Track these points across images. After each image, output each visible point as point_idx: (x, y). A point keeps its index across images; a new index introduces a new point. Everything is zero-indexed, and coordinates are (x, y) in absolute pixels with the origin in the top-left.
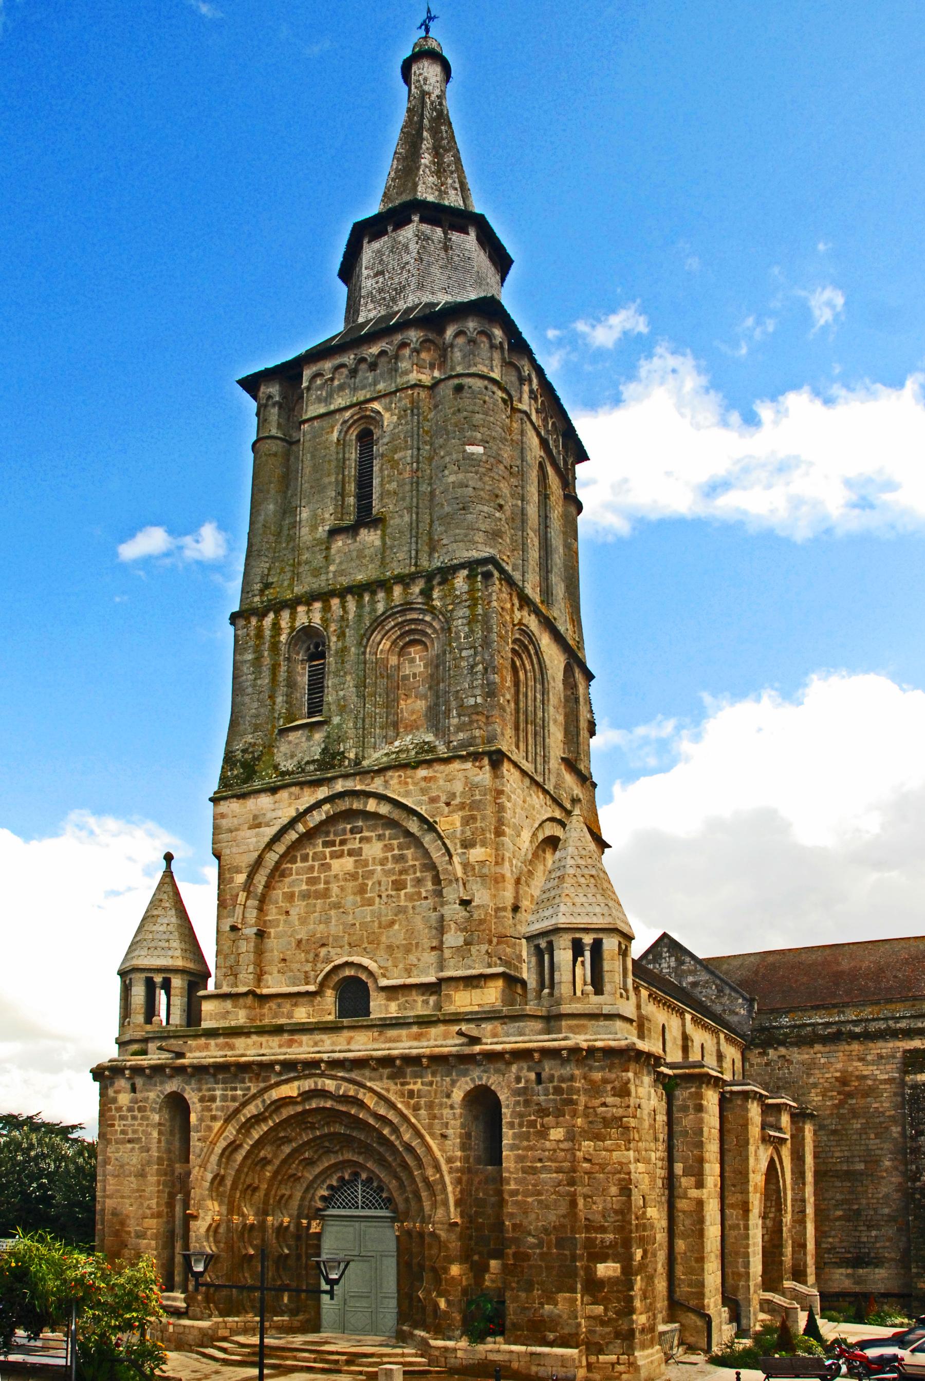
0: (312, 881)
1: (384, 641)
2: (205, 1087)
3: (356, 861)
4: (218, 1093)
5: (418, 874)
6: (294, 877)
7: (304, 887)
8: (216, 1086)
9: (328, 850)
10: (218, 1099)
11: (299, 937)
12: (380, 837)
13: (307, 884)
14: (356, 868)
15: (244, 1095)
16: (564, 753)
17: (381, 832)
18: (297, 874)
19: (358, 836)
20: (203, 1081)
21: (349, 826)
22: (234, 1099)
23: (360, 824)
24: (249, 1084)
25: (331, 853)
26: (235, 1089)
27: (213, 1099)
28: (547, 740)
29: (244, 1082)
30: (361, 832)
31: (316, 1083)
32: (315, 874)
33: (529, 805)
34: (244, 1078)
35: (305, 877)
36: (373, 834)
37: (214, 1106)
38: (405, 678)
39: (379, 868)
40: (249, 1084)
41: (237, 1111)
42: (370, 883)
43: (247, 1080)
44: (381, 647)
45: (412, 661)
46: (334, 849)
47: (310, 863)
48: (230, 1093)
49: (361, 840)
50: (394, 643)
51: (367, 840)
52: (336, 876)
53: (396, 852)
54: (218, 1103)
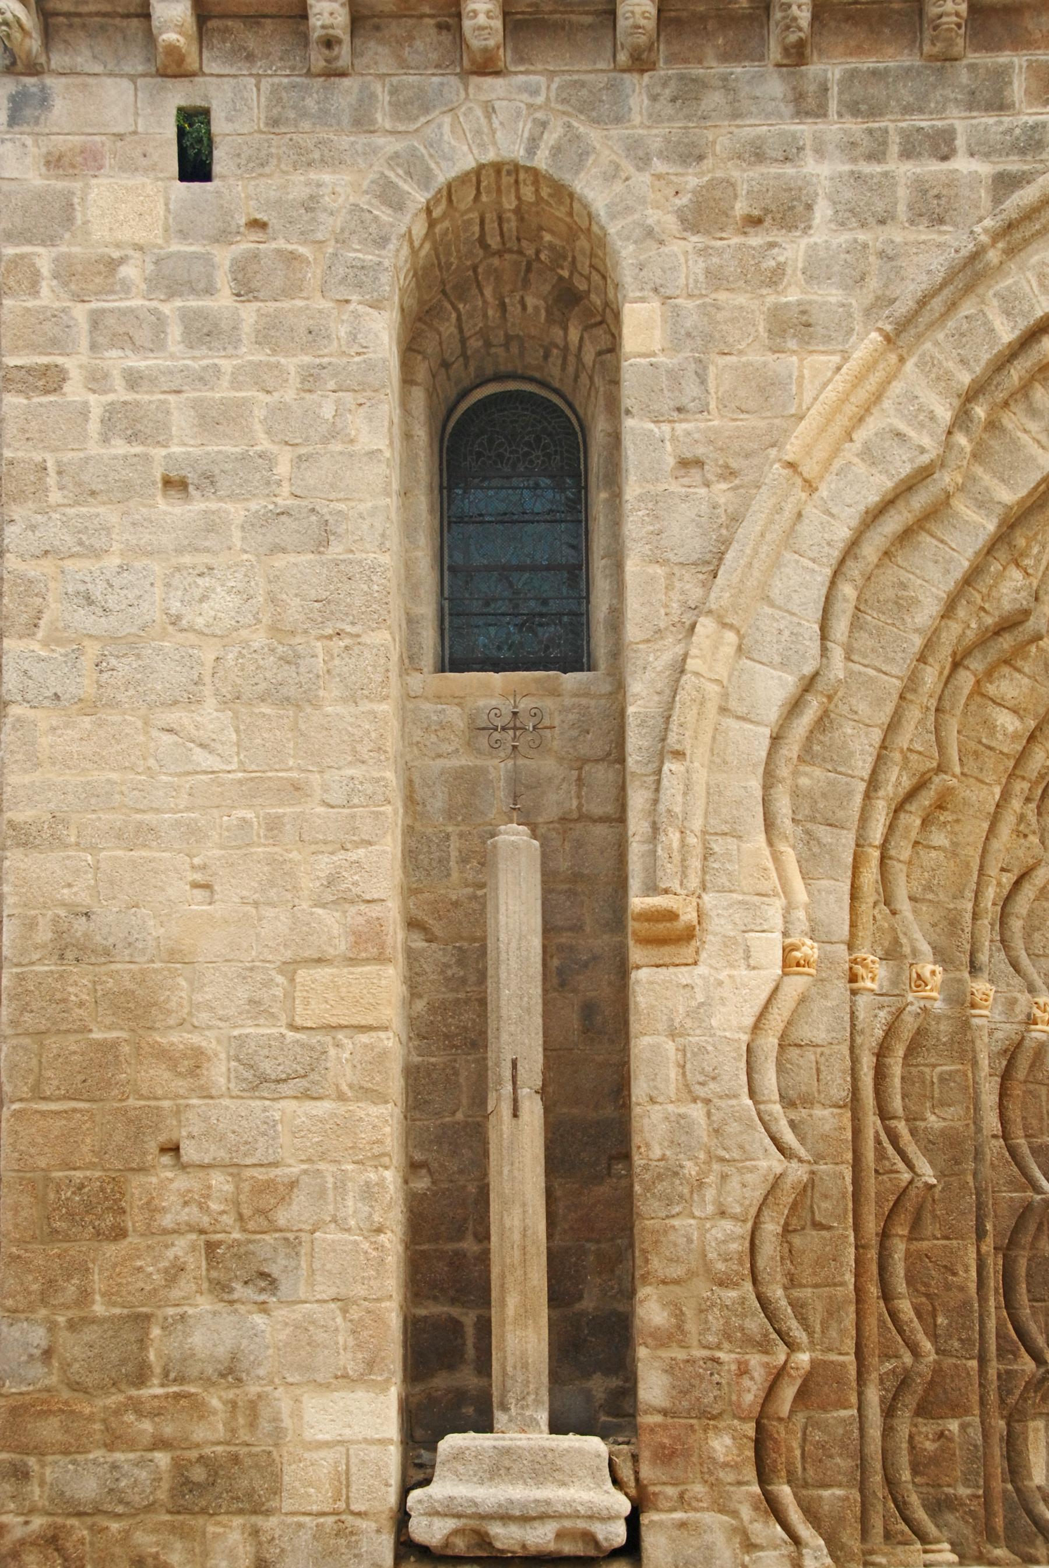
2: (722, 138)
4: (821, 172)
8: (805, 129)
10: (822, 211)
15: (1005, 183)
20: (714, 99)
22: (933, 208)
26: (942, 146)
27: (787, 212)
29: (1000, 105)
34: (1001, 76)
37: (794, 250)
41: (969, 274)
43: (1018, 88)
48: (905, 170)
54: (823, 232)
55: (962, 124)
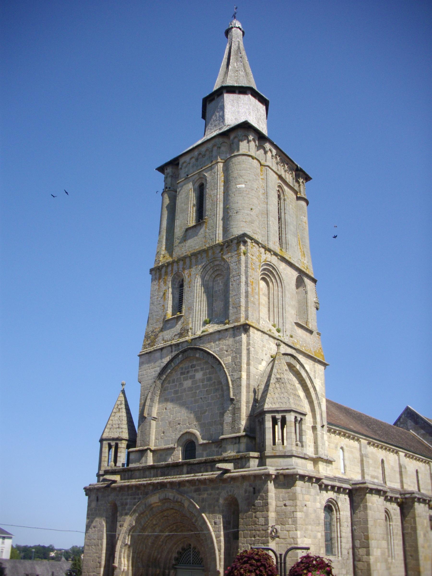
0: (176, 392)
1: (206, 276)
3: (193, 381)
5: (216, 387)
6: (169, 390)
7: (173, 395)
9: (182, 377)
11: (170, 420)
12: (202, 369)
13: (174, 394)
14: (192, 384)
16: (297, 320)
17: (202, 366)
18: (170, 389)
19: (194, 369)
21: (191, 364)
23: (195, 363)
24: (140, 496)
25: (184, 378)
27: (126, 504)
28: (284, 314)
30: (195, 367)
31: (166, 495)
32: (177, 389)
33: (268, 348)
35: (173, 390)
36: (199, 368)
38: (216, 292)
39: (201, 384)
40: (140, 496)
42: (198, 391)
44: (205, 279)
45: (219, 283)
46: (184, 376)
47: (176, 383)
49: (195, 370)
50: (211, 276)
51: (196, 371)
52: (185, 389)
53: (208, 376)
55: (137, 496)
